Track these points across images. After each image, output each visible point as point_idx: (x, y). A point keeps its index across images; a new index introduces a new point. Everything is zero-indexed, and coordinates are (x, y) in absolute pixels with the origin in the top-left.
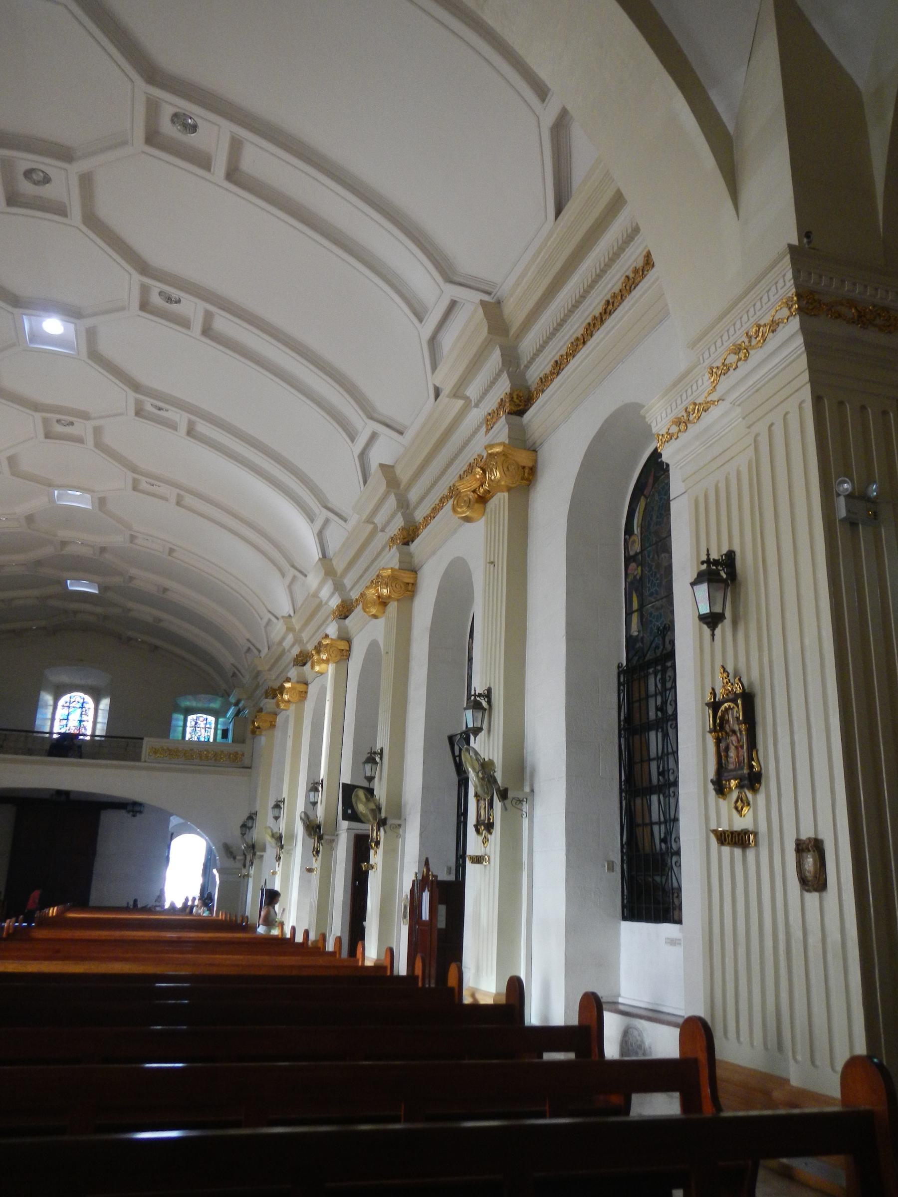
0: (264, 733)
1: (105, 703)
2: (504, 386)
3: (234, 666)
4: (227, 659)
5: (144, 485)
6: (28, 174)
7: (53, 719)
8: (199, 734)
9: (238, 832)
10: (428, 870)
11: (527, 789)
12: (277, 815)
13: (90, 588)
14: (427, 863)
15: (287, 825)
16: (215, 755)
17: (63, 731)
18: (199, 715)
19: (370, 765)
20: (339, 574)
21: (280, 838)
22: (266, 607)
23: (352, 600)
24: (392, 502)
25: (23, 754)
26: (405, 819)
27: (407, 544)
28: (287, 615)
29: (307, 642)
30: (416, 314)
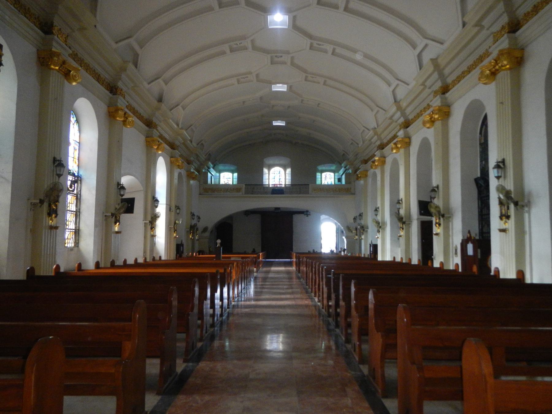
1: (289, 171)
2: (505, 20)
5: (310, 78)
7: (269, 179)
9: (352, 221)
10: (470, 235)
11: (526, 201)
12: (377, 214)
14: (469, 232)
15: (381, 219)
16: (339, 189)
19: (433, 192)
21: (379, 223)
24: (436, 75)
27: (444, 93)
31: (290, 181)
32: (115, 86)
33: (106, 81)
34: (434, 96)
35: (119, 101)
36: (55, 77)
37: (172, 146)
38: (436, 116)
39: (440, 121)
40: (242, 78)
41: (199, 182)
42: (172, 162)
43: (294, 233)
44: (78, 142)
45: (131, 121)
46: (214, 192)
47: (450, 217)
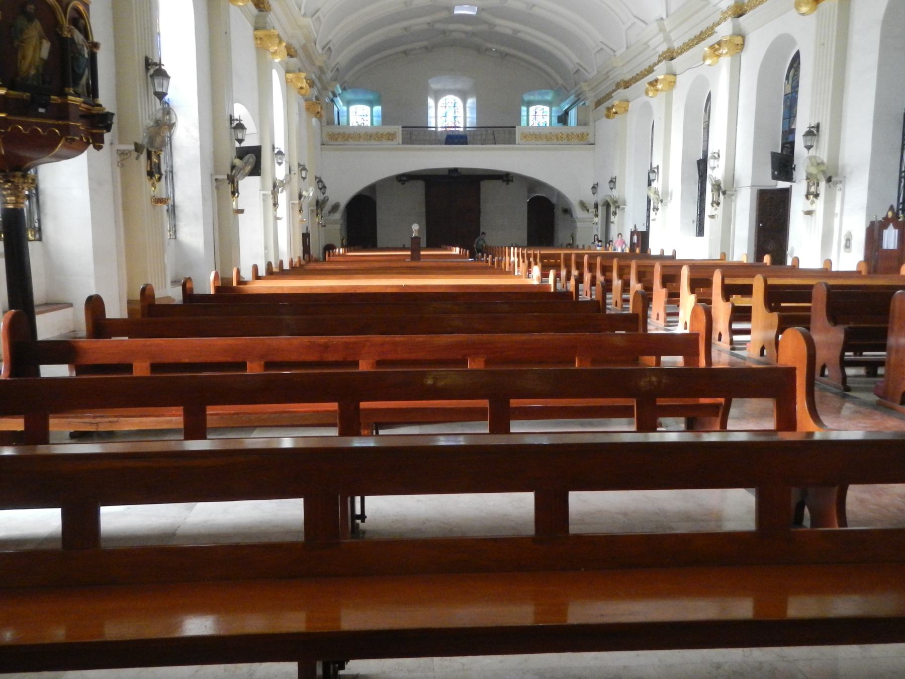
1: (471, 101)
3: (581, 66)
4: (570, 58)
7: (436, 117)
9: (590, 192)
13: (470, 11)
19: (809, 137)
21: (658, 195)
22: (632, 13)
25: (436, 144)
26: (845, 177)
28: (659, 18)
29: (674, 41)
42: (289, 80)
43: (482, 215)
46: (347, 140)
47: (836, 183)
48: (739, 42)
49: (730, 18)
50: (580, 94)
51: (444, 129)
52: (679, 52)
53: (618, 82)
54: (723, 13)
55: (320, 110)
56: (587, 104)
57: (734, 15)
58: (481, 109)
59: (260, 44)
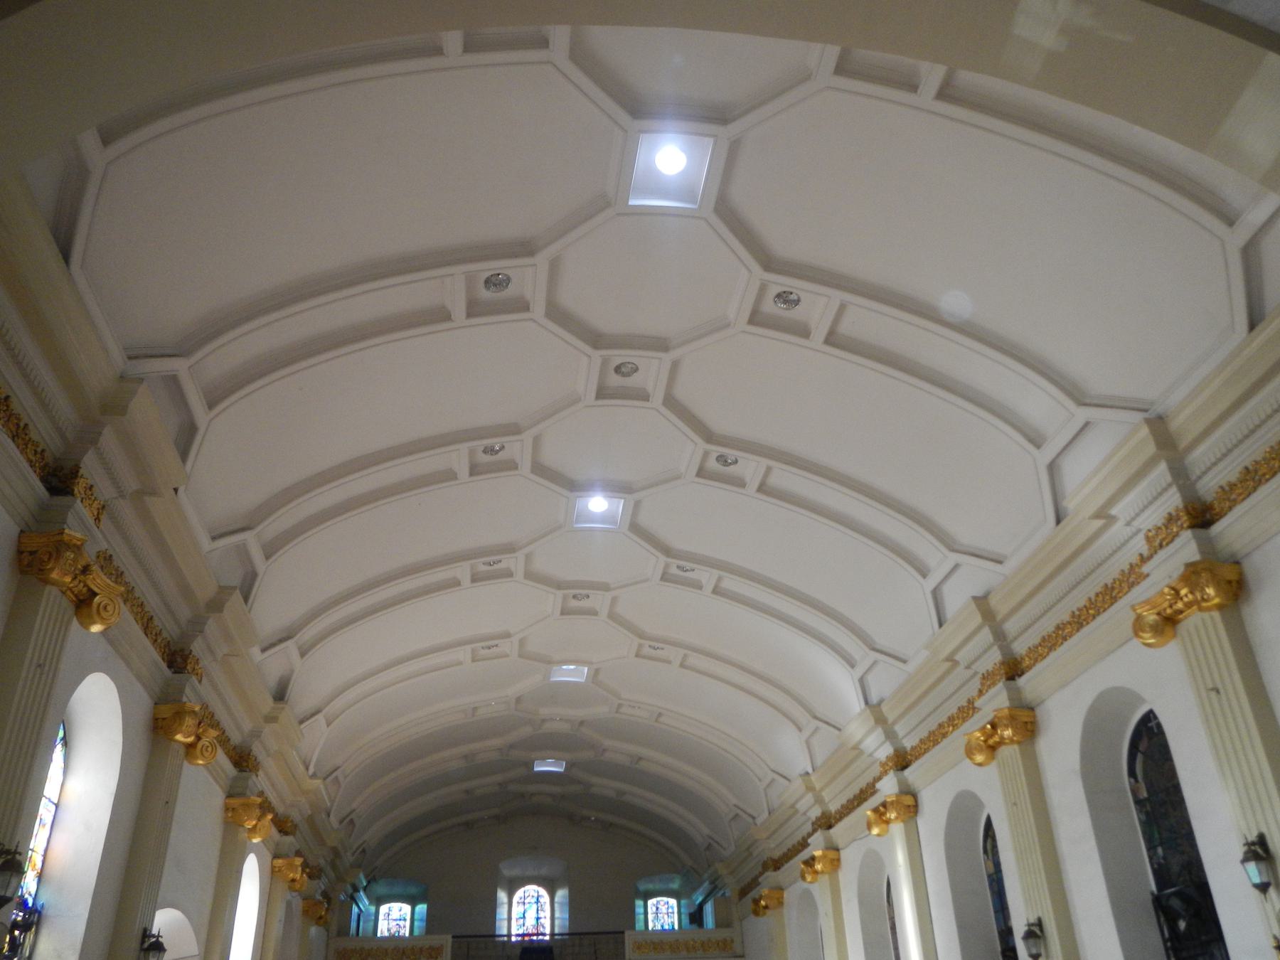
0: (769, 912)
1: (562, 894)
2: (1173, 500)
3: (710, 837)
4: (698, 829)
6: (618, 370)
8: (662, 921)
16: (703, 944)
17: (521, 932)
18: (659, 899)
19: (1031, 941)
20: (889, 723)
22: (768, 766)
23: (905, 748)
24: (986, 635)
29: (831, 801)
30: (1031, 441)
31: (567, 923)
32: (182, 650)
33: (165, 634)
34: (982, 684)
35: (188, 690)
36: (52, 602)
37: (283, 826)
38: (1008, 733)
39: (1016, 747)
40: (483, 648)
41: (327, 931)
44: (56, 802)
45: (208, 747)
48: (909, 805)
49: (892, 771)
50: (716, 879)
51: (519, 939)
52: (838, 816)
53: (764, 862)
54: (883, 765)
55: (323, 913)
56: (727, 895)
57: (896, 766)
58: (575, 906)
59: (232, 817)
